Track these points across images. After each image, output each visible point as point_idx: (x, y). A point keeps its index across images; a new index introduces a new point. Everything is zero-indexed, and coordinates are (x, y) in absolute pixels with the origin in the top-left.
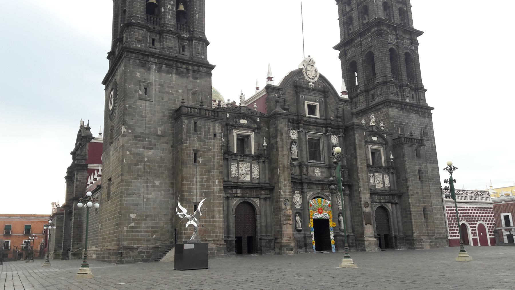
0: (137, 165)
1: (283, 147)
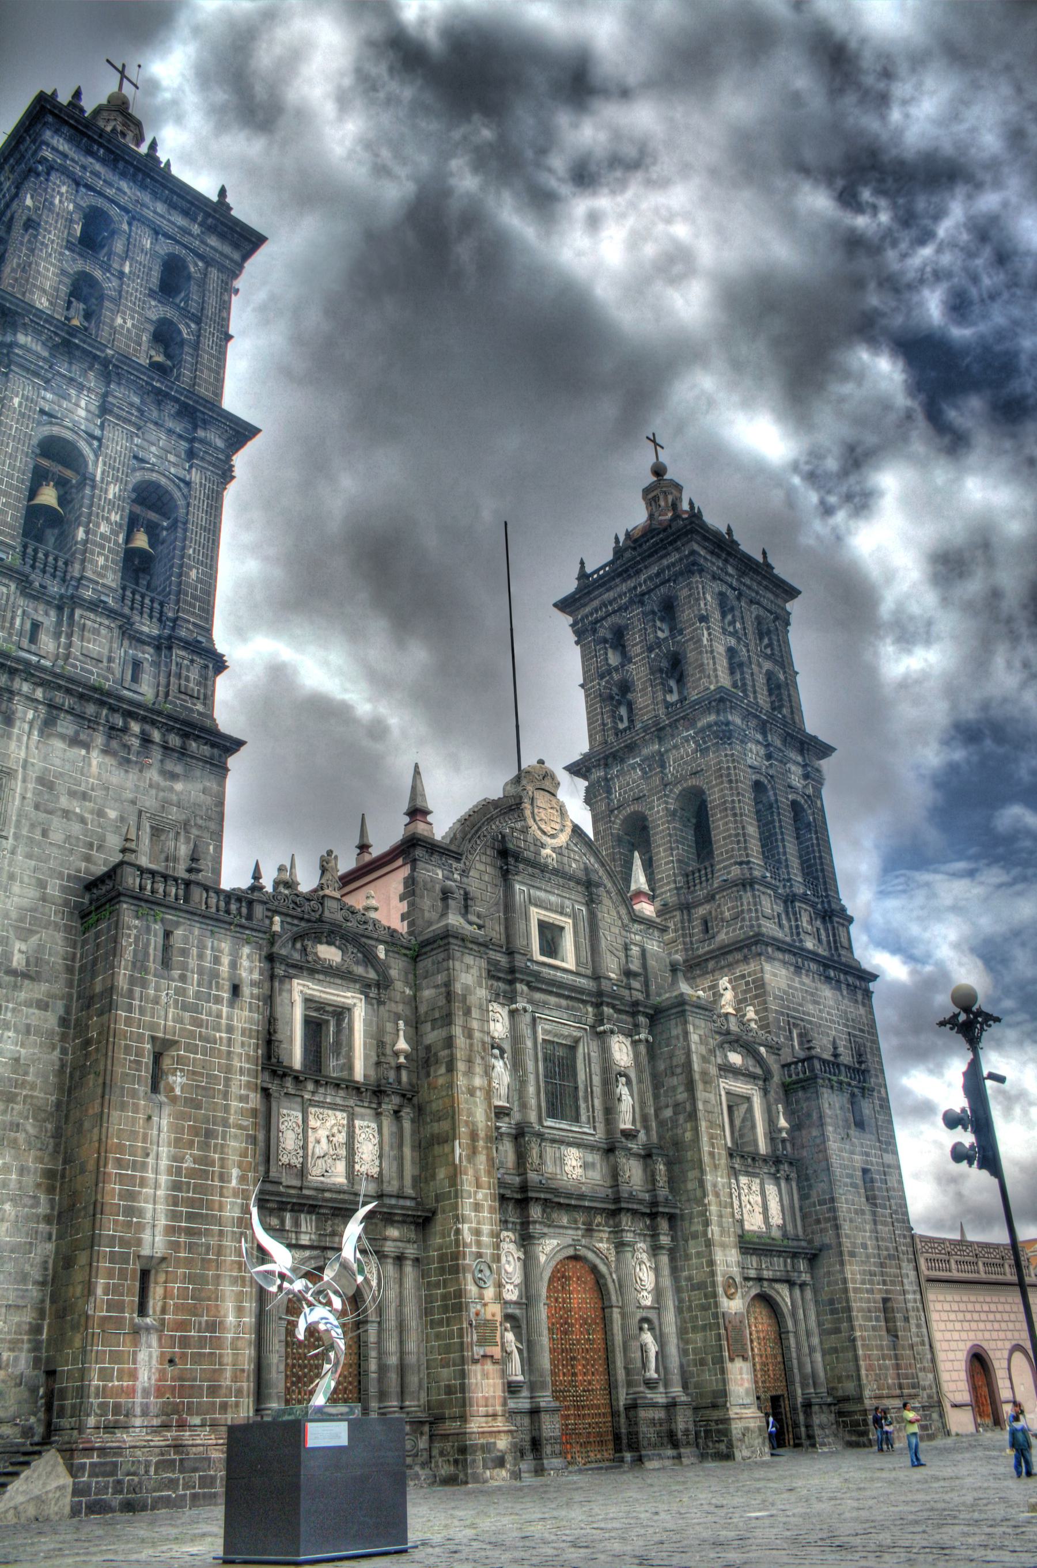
1: (470, 1061)
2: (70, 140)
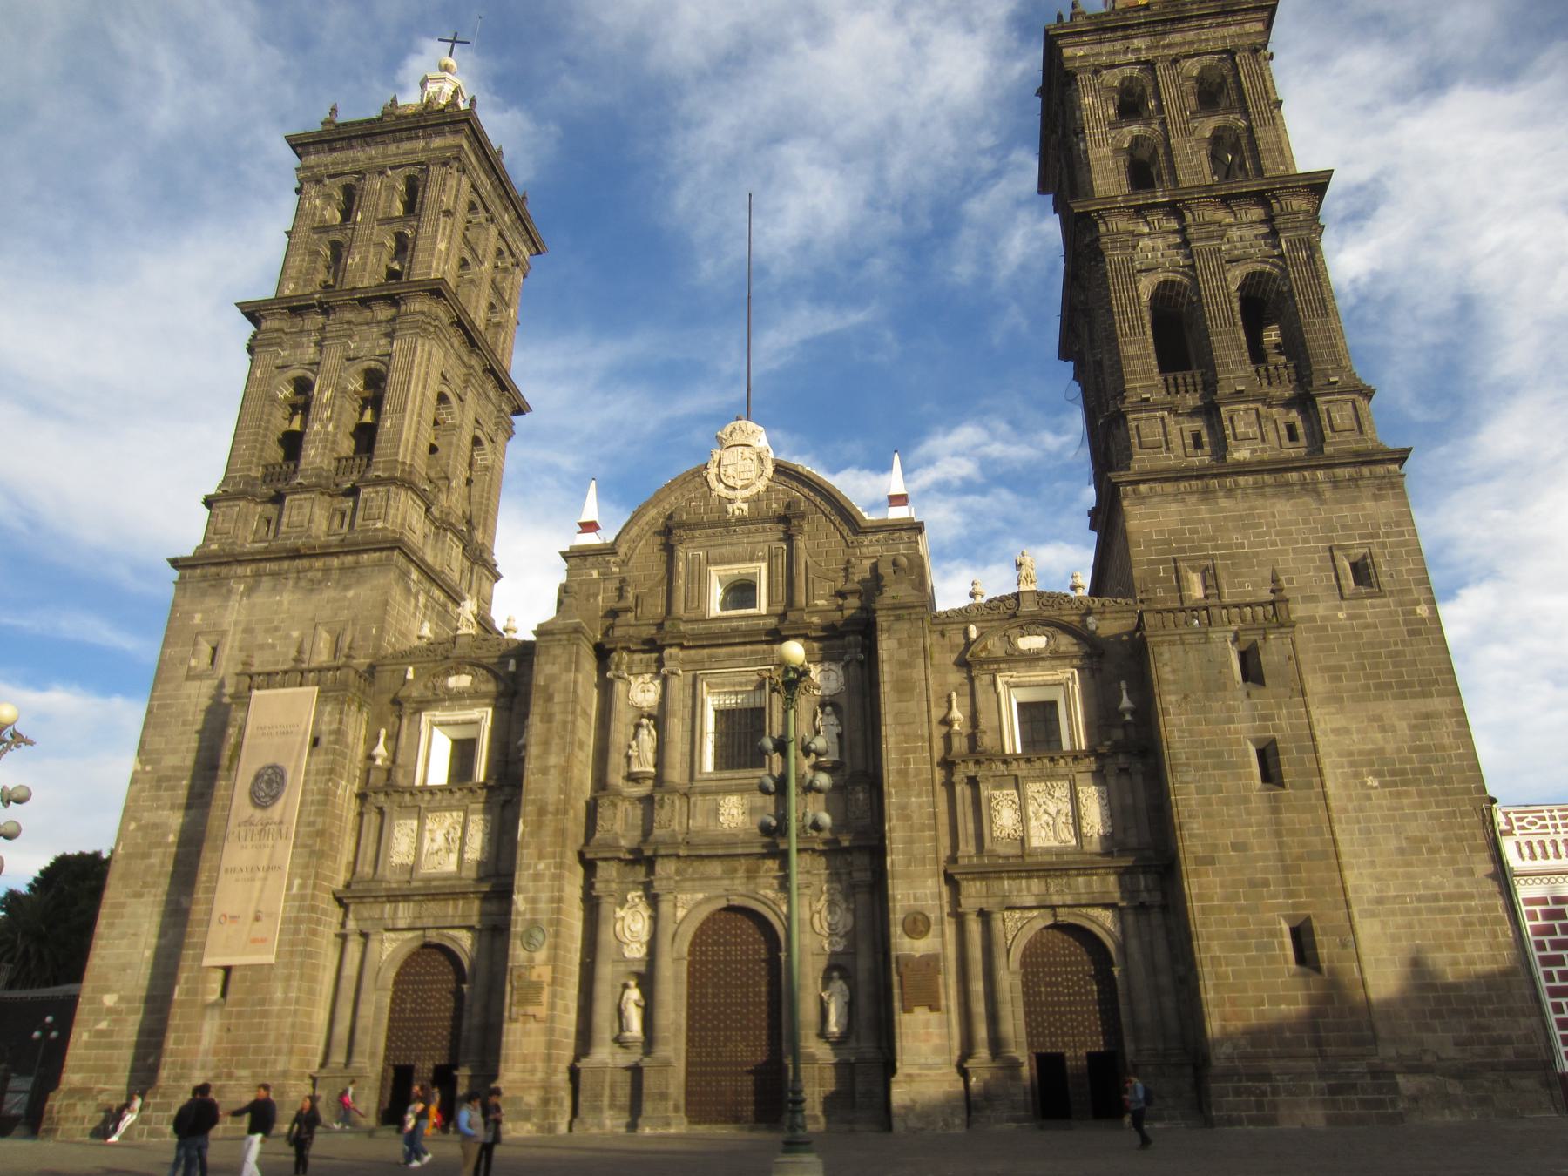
0: (146, 856)
1: (546, 743)
2: (317, 152)
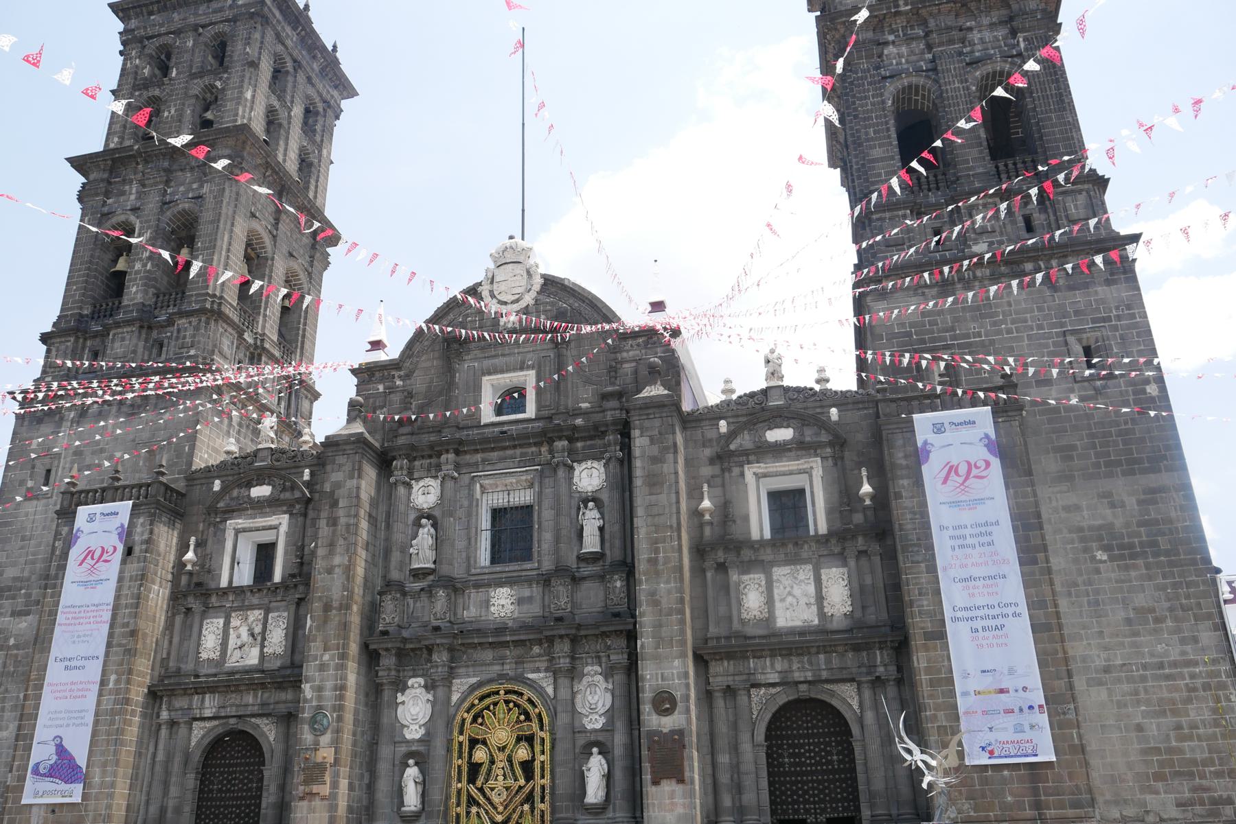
1: (332, 545)
